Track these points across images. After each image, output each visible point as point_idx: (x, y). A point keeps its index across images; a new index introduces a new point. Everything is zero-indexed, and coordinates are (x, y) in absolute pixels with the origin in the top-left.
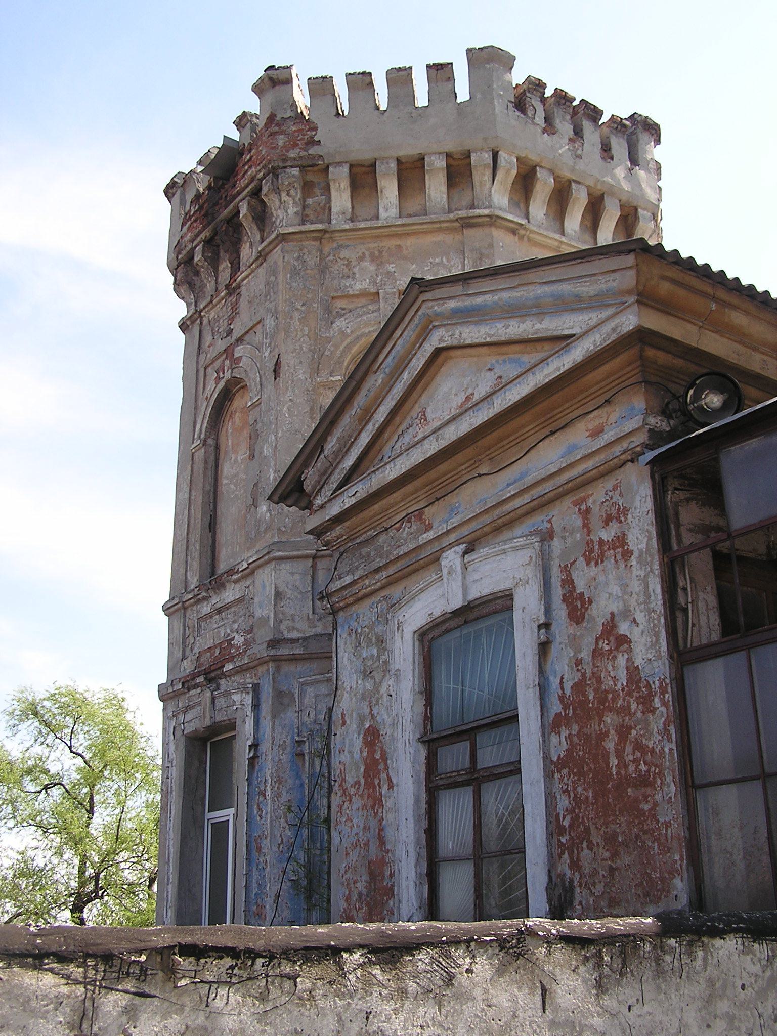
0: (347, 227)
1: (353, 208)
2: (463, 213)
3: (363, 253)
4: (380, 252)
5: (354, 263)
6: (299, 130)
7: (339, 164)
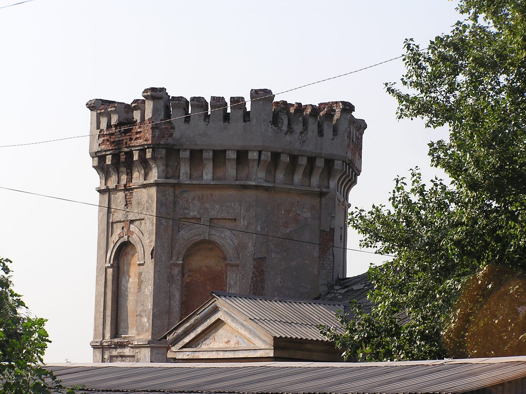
0: (187, 182)
1: (190, 170)
2: (242, 183)
3: (195, 196)
4: (203, 196)
5: (190, 201)
6: (166, 128)
7: (185, 150)
